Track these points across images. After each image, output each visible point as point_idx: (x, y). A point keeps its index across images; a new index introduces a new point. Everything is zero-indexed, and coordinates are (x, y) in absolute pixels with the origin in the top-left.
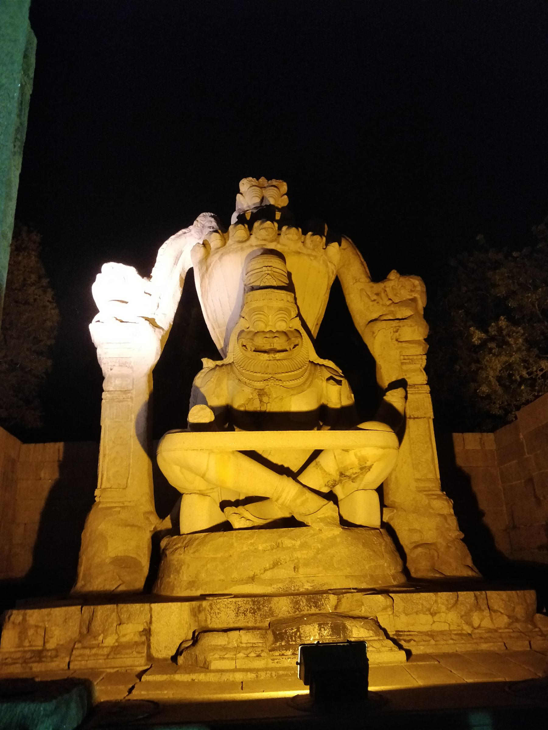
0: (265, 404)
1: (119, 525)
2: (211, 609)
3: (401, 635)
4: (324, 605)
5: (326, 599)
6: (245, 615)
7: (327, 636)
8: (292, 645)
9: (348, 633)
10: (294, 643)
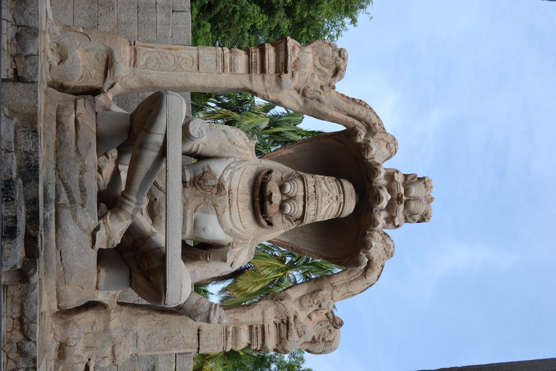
0: (210, 190)
2: (32, 132)
3: (3, 288)
4: (31, 226)
5: (36, 228)
6: (26, 159)
7: (6, 223)
9: (8, 240)
10: (2, 195)
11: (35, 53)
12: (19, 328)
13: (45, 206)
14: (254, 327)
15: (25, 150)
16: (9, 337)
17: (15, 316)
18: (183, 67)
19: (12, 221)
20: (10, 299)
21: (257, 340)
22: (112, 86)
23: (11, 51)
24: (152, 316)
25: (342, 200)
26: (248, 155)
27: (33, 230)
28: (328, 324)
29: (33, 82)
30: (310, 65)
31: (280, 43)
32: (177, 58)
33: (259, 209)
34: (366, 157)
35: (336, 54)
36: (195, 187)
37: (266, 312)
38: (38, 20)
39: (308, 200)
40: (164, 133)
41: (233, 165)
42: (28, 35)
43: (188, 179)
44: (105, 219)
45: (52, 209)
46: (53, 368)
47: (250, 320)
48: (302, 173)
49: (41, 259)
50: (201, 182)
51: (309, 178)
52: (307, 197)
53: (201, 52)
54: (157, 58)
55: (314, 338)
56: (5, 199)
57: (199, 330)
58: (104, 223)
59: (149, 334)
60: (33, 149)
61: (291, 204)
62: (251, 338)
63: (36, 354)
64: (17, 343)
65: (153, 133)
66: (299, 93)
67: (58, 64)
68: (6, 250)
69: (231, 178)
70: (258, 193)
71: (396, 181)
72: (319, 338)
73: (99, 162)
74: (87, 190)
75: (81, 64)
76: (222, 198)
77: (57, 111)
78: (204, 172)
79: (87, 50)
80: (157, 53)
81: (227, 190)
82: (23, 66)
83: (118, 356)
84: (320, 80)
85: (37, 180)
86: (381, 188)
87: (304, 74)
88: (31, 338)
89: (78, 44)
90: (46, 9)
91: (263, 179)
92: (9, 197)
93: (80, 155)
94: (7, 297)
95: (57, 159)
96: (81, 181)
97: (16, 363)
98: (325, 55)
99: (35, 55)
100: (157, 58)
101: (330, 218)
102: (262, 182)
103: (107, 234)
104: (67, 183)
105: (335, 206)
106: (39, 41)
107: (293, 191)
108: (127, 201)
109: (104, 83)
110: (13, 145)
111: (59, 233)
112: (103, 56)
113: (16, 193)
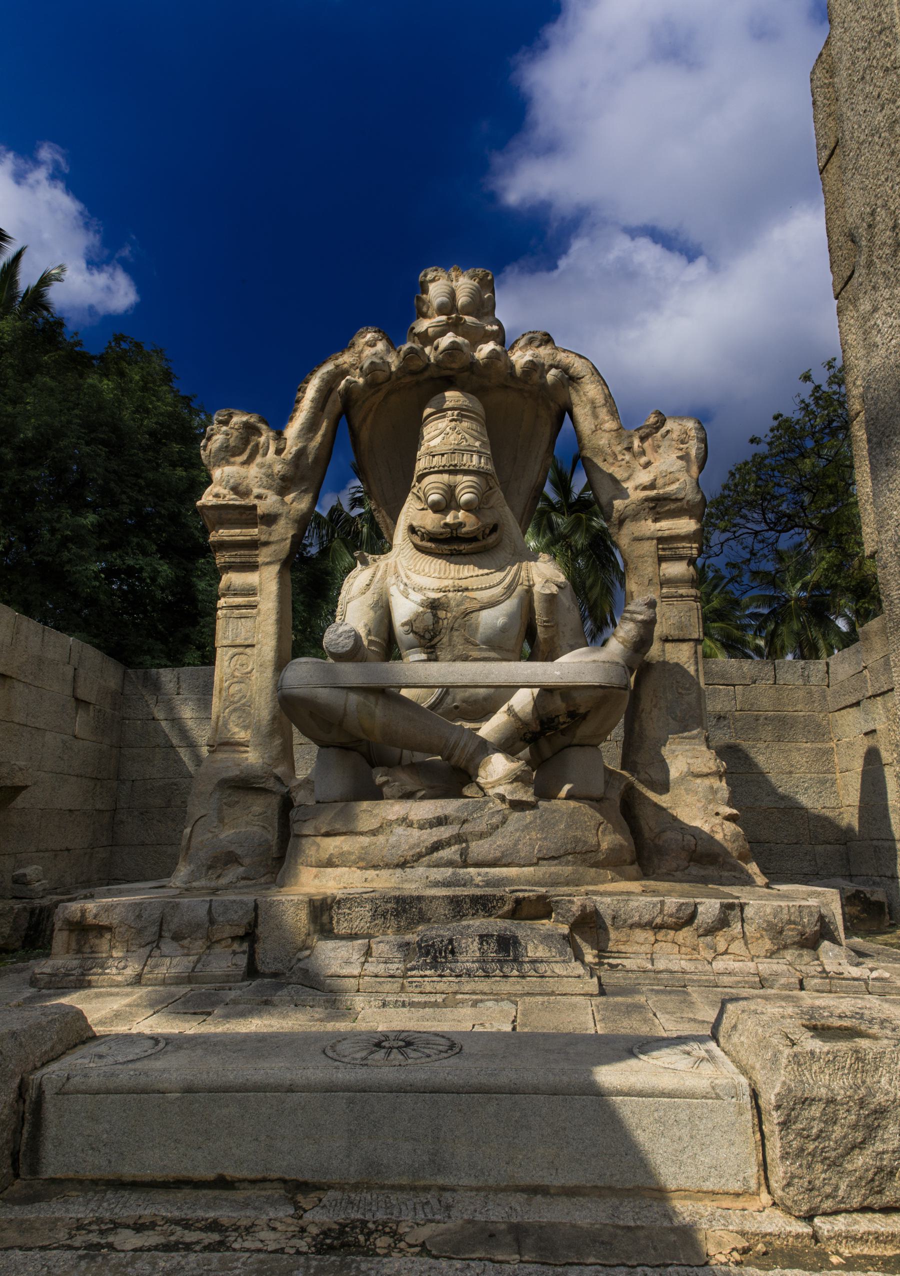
1: (239, 788)
8: (441, 962)
10: (443, 960)
11: (207, 906)
12: (672, 933)
13: (464, 885)
14: (661, 553)
15: (369, 919)
16: (689, 950)
17: (652, 939)
18: (249, 669)
19: (487, 943)
20: (622, 947)
21: (684, 548)
22: (278, 779)
23: (202, 948)
24: (643, 715)
25: (456, 412)
26: (387, 565)
27: (504, 905)
28: (659, 434)
29: (256, 908)
30: (243, 470)
31: (207, 517)
32: (236, 680)
33: (473, 545)
34: (388, 373)
35: (224, 428)
36: (436, 644)
37: (636, 534)
38: (151, 903)
39: (455, 465)
40: (345, 691)
41: (402, 587)
42: (176, 920)
43: (424, 656)
44: (486, 786)
45: (469, 874)
46: (733, 874)
47: (650, 560)
48: (415, 479)
49: (552, 891)
50: (427, 636)
51: (421, 465)
52: (452, 468)
53: (226, 642)
54: (235, 710)
55: (680, 458)
56: (450, 956)
57: (666, 640)
58: (493, 787)
59: (673, 718)
60: (368, 907)
61: (463, 492)
62: (680, 558)
63: (716, 903)
64: (699, 936)
65: (345, 709)
66: (289, 488)
67: (242, 866)
68: (537, 955)
69: (420, 590)
70: (446, 547)
71: (427, 330)
72: (681, 450)
73: (392, 797)
74: (437, 815)
75: (243, 830)
76: (453, 603)
77: (311, 866)
78: (412, 631)
79: (221, 820)
80: (227, 710)
81: (442, 594)
82: (228, 927)
83: (710, 768)
84: (266, 454)
85: (419, 898)
86: (436, 348)
87: (256, 480)
88: (689, 911)
89: (210, 835)
90: (151, 888)
91: (422, 539)
92: (447, 948)
93: (381, 827)
94: (618, 952)
95: (387, 866)
96: (421, 828)
97: (733, 939)
98: (227, 447)
99: (210, 906)
100: (235, 710)
101: (485, 433)
102: (428, 541)
103: (512, 783)
104: (427, 848)
105: (465, 424)
106: (186, 900)
107: (442, 489)
108: (457, 752)
109: (274, 793)
110: (360, 941)
111: (510, 861)
112: (230, 795)
113: (439, 936)
